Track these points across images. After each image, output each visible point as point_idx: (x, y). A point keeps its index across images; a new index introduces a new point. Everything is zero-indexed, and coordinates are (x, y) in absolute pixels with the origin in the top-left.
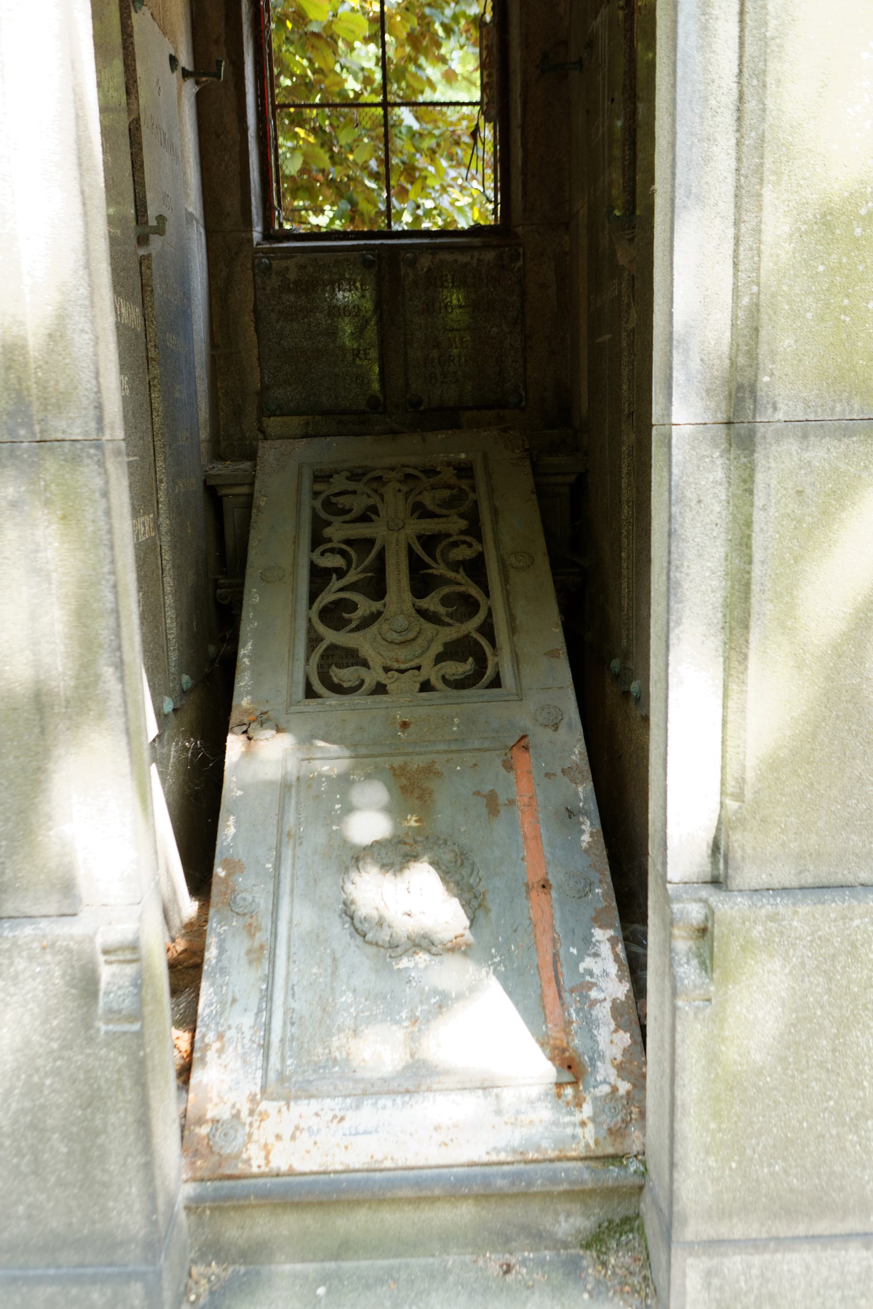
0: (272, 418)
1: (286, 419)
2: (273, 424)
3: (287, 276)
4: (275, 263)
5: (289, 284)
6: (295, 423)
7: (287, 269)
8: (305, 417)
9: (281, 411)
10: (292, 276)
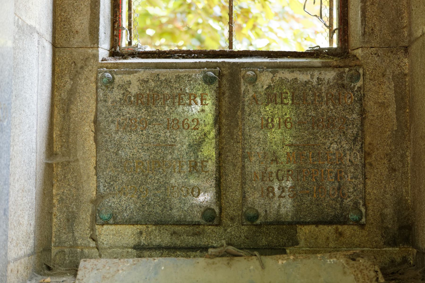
0: (105, 227)
1: (119, 227)
2: (107, 234)
3: (129, 89)
4: (117, 78)
5: (130, 97)
6: (128, 234)
7: (129, 83)
8: (139, 227)
9: (114, 220)
10: (134, 90)
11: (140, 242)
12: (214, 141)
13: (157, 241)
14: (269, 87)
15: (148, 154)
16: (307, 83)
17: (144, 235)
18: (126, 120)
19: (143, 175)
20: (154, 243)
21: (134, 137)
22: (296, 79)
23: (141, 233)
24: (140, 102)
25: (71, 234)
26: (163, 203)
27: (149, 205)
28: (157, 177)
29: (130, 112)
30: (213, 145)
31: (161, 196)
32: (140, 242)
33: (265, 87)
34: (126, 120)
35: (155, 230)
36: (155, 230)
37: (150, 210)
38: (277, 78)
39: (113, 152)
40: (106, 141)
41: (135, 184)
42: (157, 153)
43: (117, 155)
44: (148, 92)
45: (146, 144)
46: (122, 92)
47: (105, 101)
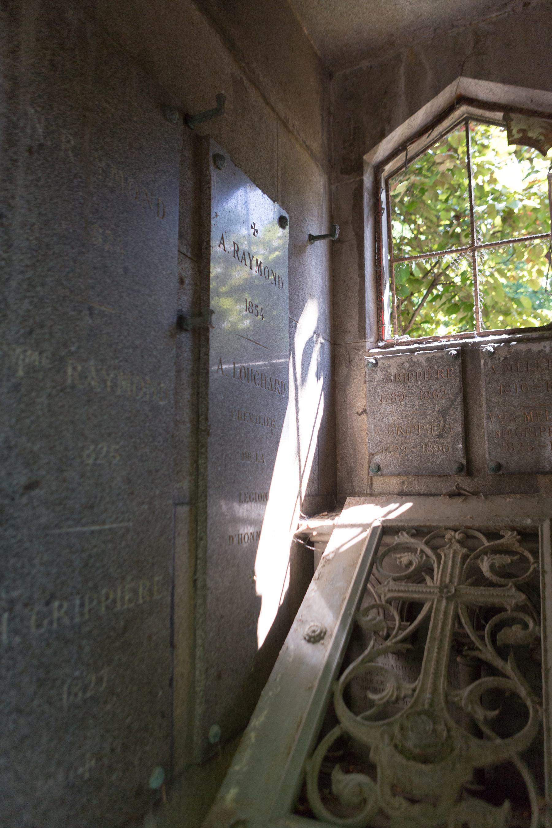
3: (389, 371)
5: (390, 377)
8: (402, 478)
10: (393, 371)
11: (402, 490)
12: (460, 406)
13: (417, 489)
14: (506, 358)
15: (406, 420)
16: (540, 352)
17: (406, 484)
18: (388, 394)
19: (402, 437)
20: (414, 491)
21: (394, 407)
22: (530, 349)
23: (403, 483)
24: (398, 380)
25: (350, 484)
26: (419, 458)
27: (408, 460)
28: (413, 438)
29: (391, 388)
30: (459, 410)
31: (418, 453)
32: (402, 490)
33: (502, 359)
34: (388, 394)
35: (415, 480)
36: (415, 480)
37: (409, 464)
38: (513, 351)
39: (379, 420)
40: (374, 412)
41: (397, 444)
42: (412, 419)
43: (382, 422)
44: (404, 371)
45: (404, 412)
46: (384, 373)
47: (372, 381)
